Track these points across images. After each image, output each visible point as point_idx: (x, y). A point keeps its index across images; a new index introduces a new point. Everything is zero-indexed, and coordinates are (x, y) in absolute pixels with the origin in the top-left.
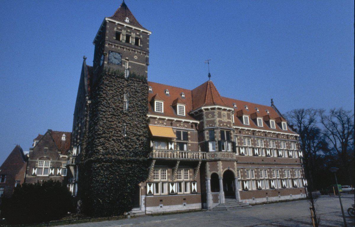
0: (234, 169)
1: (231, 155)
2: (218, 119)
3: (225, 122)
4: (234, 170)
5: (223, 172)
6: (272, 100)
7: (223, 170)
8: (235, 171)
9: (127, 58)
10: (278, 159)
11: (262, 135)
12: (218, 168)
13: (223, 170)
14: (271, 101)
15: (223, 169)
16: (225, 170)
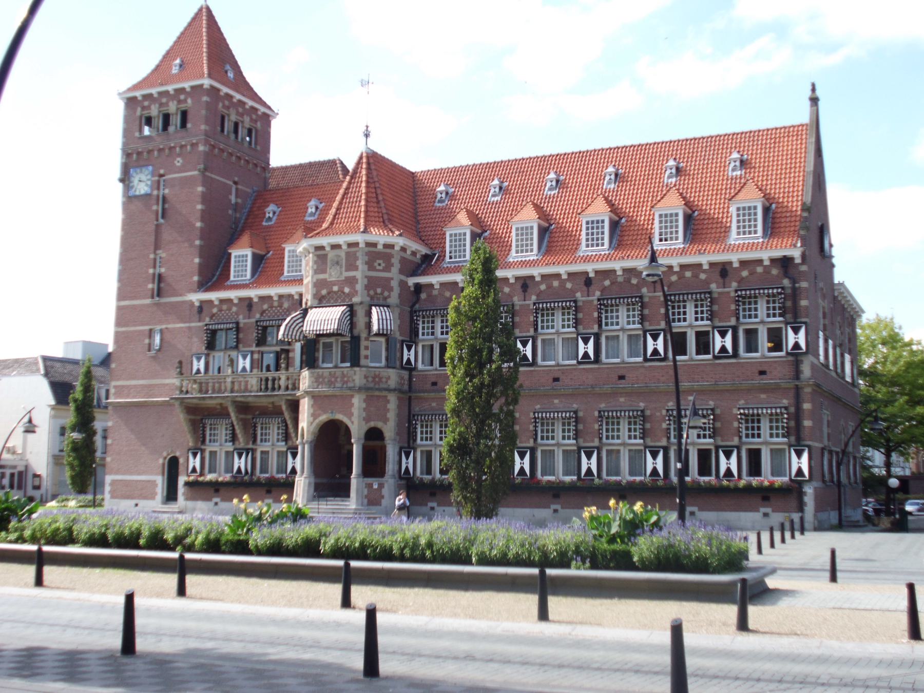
0: (350, 415)
1: (343, 375)
2: (358, 274)
3: (333, 283)
4: (350, 419)
5: (314, 424)
6: (813, 86)
7: (314, 419)
8: (352, 423)
9: (162, 172)
10: (643, 367)
11: (569, 285)
12: (364, 415)
13: (314, 419)
14: (809, 93)
15: (314, 416)
16: (324, 418)
